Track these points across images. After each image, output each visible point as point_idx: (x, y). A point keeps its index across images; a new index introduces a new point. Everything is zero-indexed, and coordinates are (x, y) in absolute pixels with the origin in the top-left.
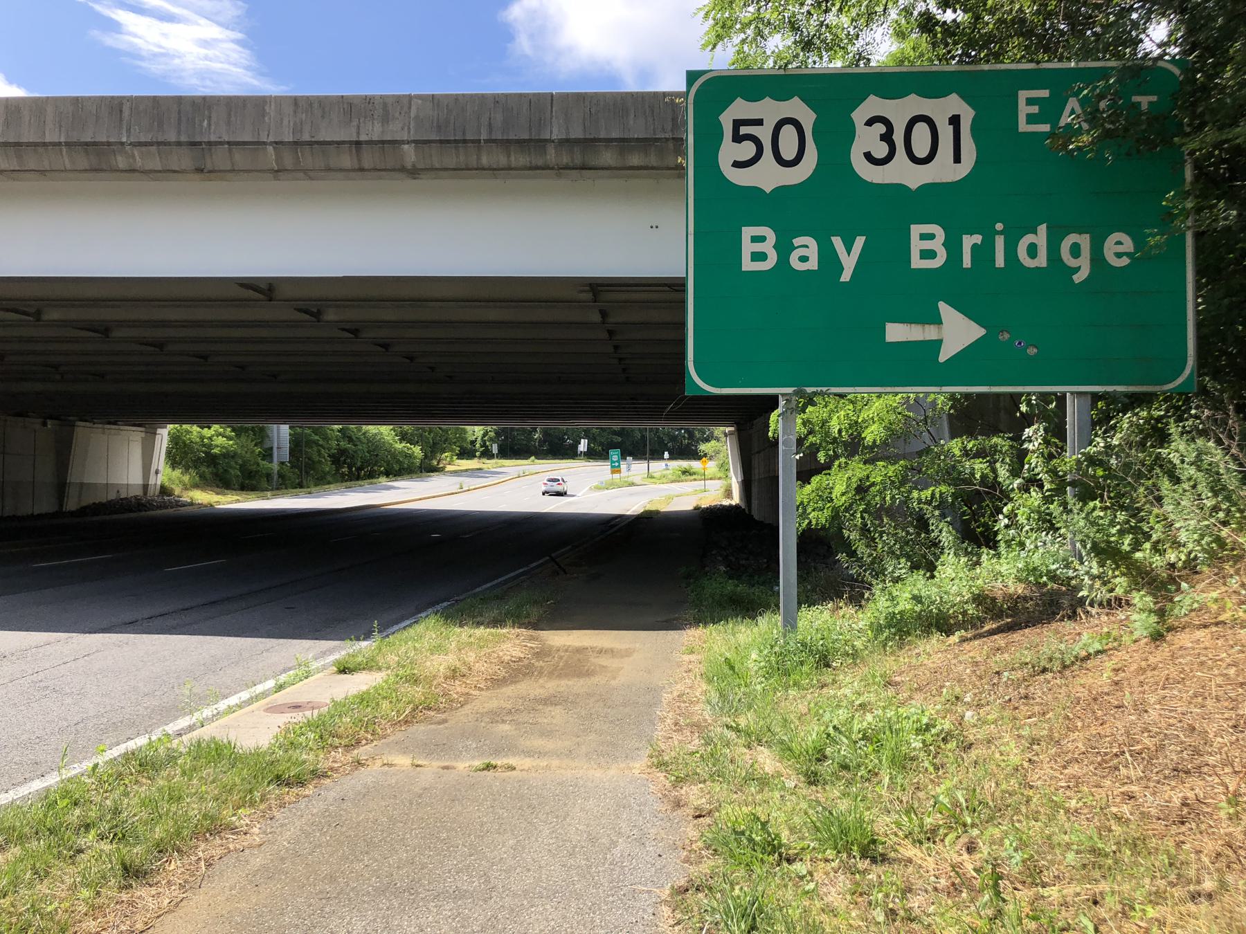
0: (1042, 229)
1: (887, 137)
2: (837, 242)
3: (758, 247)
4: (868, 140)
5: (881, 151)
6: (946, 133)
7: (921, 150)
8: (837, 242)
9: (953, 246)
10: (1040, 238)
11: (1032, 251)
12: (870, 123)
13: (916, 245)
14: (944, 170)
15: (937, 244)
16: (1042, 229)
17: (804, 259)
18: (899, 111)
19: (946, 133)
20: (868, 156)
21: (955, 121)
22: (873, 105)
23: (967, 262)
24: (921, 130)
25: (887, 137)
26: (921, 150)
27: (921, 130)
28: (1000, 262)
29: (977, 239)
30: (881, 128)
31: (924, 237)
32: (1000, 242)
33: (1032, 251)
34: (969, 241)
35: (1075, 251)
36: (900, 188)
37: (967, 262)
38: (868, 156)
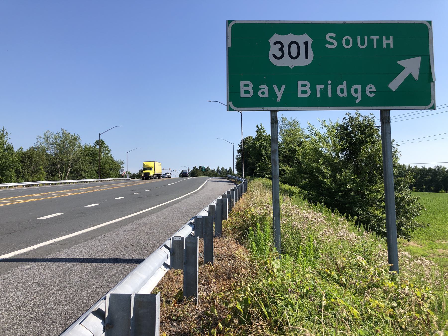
0: (345, 83)
1: (281, 49)
2: (275, 87)
3: (246, 89)
4: (274, 50)
5: (279, 54)
6: (303, 48)
7: (294, 54)
8: (275, 87)
9: (313, 89)
10: (344, 86)
11: (342, 91)
12: (275, 43)
13: (300, 88)
14: (302, 62)
15: (307, 88)
16: (345, 83)
17: (263, 93)
18: (286, 39)
20: (274, 56)
22: (276, 37)
23: (318, 95)
24: (294, 46)
25: (281, 49)
26: (294, 54)
27: (294, 46)
28: (330, 95)
29: (322, 86)
30: (279, 46)
31: (303, 85)
32: (330, 87)
33: (342, 91)
34: (319, 87)
35: (356, 91)
37: (318, 95)
38: (274, 56)
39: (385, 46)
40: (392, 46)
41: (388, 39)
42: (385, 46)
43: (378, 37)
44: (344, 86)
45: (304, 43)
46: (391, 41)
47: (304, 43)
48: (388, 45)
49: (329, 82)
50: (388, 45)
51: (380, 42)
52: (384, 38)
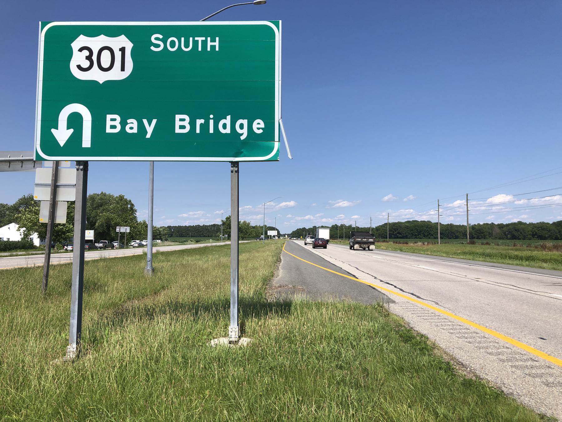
0: (229, 117)
1: (89, 58)
4: (78, 59)
5: (86, 64)
6: (118, 55)
7: (106, 63)
10: (228, 120)
11: (225, 126)
12: (81, 50)
16: (229, 117)
18: (96, 43)
19: (118, 55)
20: (79, 67)
21: (123, 50)
24: (106, 55)
26: (106, 63)
27: (106, 55)
30: (86, 53)
32: (211, 122)
33: (225, 126)
36: (95, 83)
38: (79, 67)
39: (209, 49)
40: (217, 49)
41: (213, 40)
42: (209, 49)
43: (204, 39)
44: (228, 120)
45: (120, 50)
46: (217, 44)
47: (120, 50)
48: (213, 47)
49: (211, 116)
50: (213, 47)
51: (204, 43)
52: (209, 39)
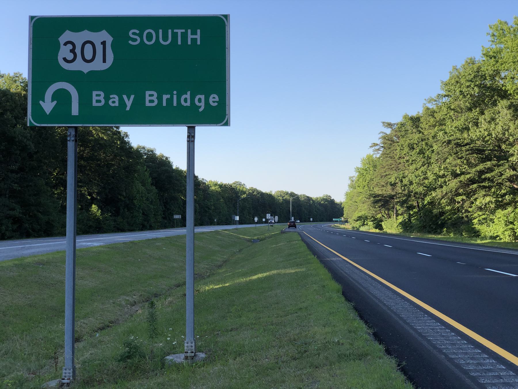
4: (65, 52)
5: (70, 57)
7: (89, 56)
20: (65, 59)
21: (104, 43)
23: (164, 104)
24: (88, 48)
26: (89, 56)
27: (88, 48)
37: (164, 104)
38: (65, 59)
41: (194, 33)
43: (183, 31)
46: (198, 37)
48: (194, 40)
50: (194, 40)
51: (184, 36)
52: (189, 31)
